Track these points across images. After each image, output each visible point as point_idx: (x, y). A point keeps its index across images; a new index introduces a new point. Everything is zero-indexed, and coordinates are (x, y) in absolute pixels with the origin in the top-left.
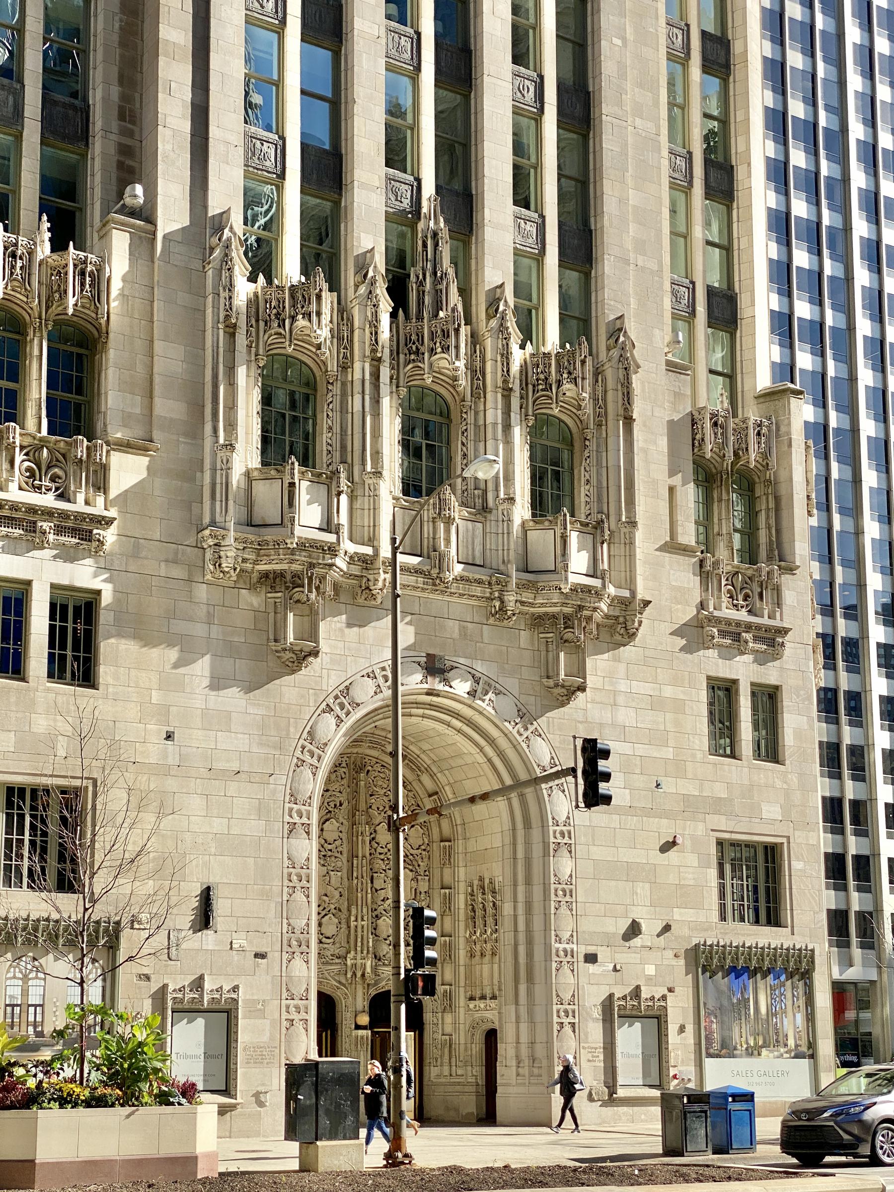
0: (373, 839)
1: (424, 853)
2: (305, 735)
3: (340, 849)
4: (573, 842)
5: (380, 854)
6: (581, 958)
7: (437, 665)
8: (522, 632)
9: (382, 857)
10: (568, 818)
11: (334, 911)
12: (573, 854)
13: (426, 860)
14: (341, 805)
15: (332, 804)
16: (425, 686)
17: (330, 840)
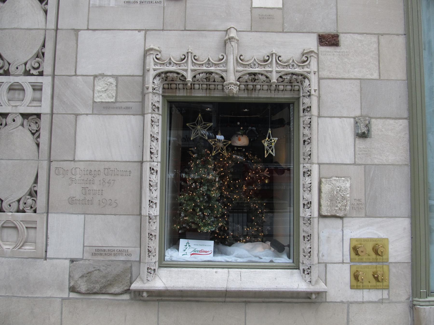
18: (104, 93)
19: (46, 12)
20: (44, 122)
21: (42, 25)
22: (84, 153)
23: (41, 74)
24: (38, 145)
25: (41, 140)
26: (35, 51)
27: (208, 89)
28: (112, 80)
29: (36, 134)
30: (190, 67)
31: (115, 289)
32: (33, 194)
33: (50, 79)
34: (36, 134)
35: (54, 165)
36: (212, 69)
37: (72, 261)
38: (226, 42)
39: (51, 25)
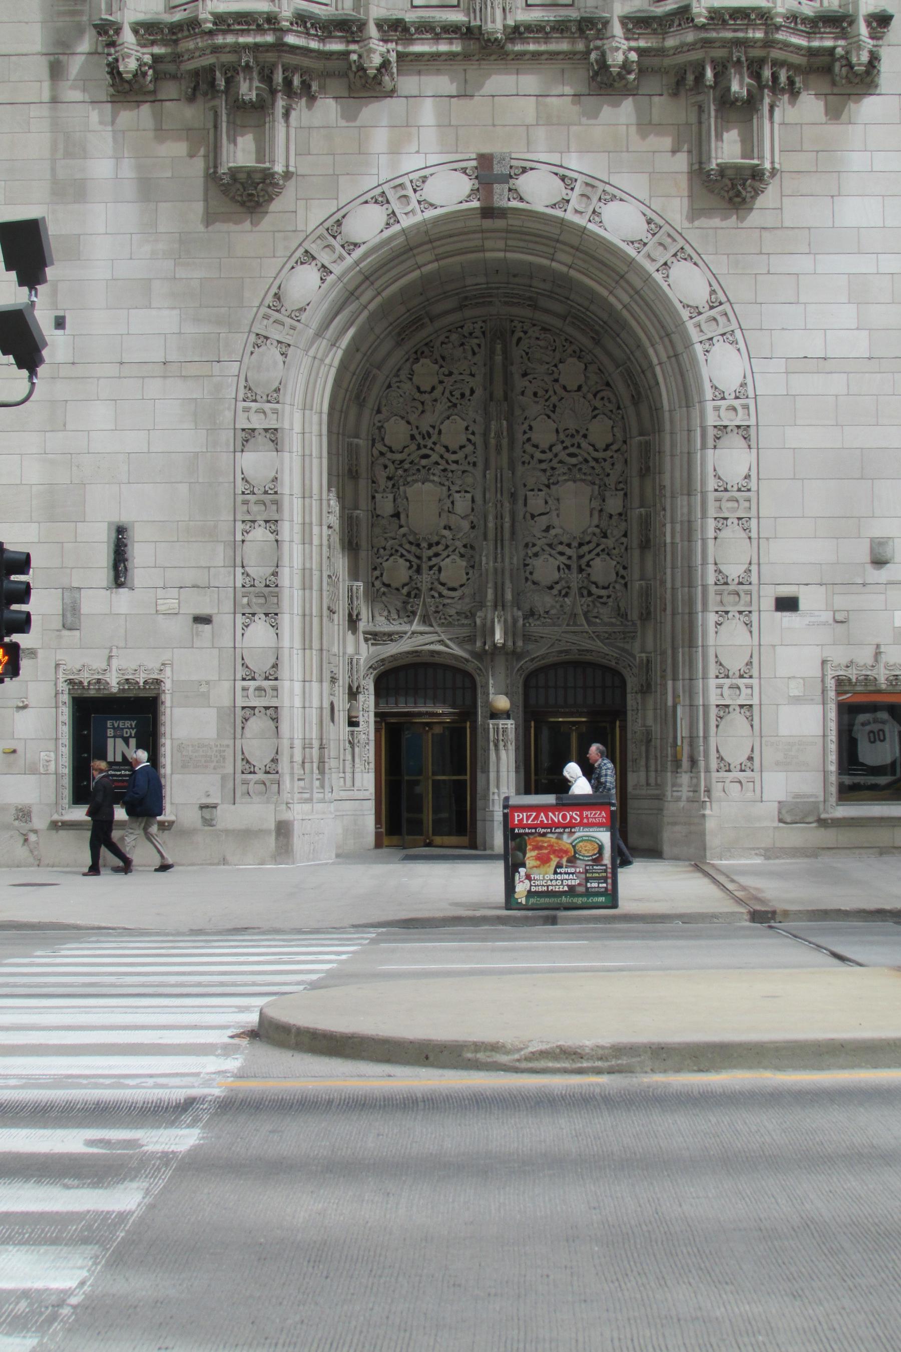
0: (529, 440)
1: (615, 455)
2: (269, 299)
3: (471, 459)
4: (752, 422)
5: (541, 461)
6: (768, 603)
7: (497, 169)
8: (656, 99)
9: (544, 466)
10: (743, 385)
11: (463, 550)
12: (753, 443)
13: (619, 467)
14: (472, 392)
15: (457, 394)
16: (476, 204)
17: (453, 446)
18: (795, 689)
19: (751, 632)
20: (756, 709)
21: (750, 643)
22: (783, 731)
23: (751, 677)
24: (752, 726)
25: (754, 723)
26: (746, 661)
27: (866, 685)
28: (801, 681)
29: (750, 719)
30: (855, 672)
31: (810, 819)
32: (750, 759)
33: (757, 680)
34: (750, 719)
35: (764, 739)
36: (869, 673)
37: (779, 802)
38: (877, 654)
39: (756, 642)
